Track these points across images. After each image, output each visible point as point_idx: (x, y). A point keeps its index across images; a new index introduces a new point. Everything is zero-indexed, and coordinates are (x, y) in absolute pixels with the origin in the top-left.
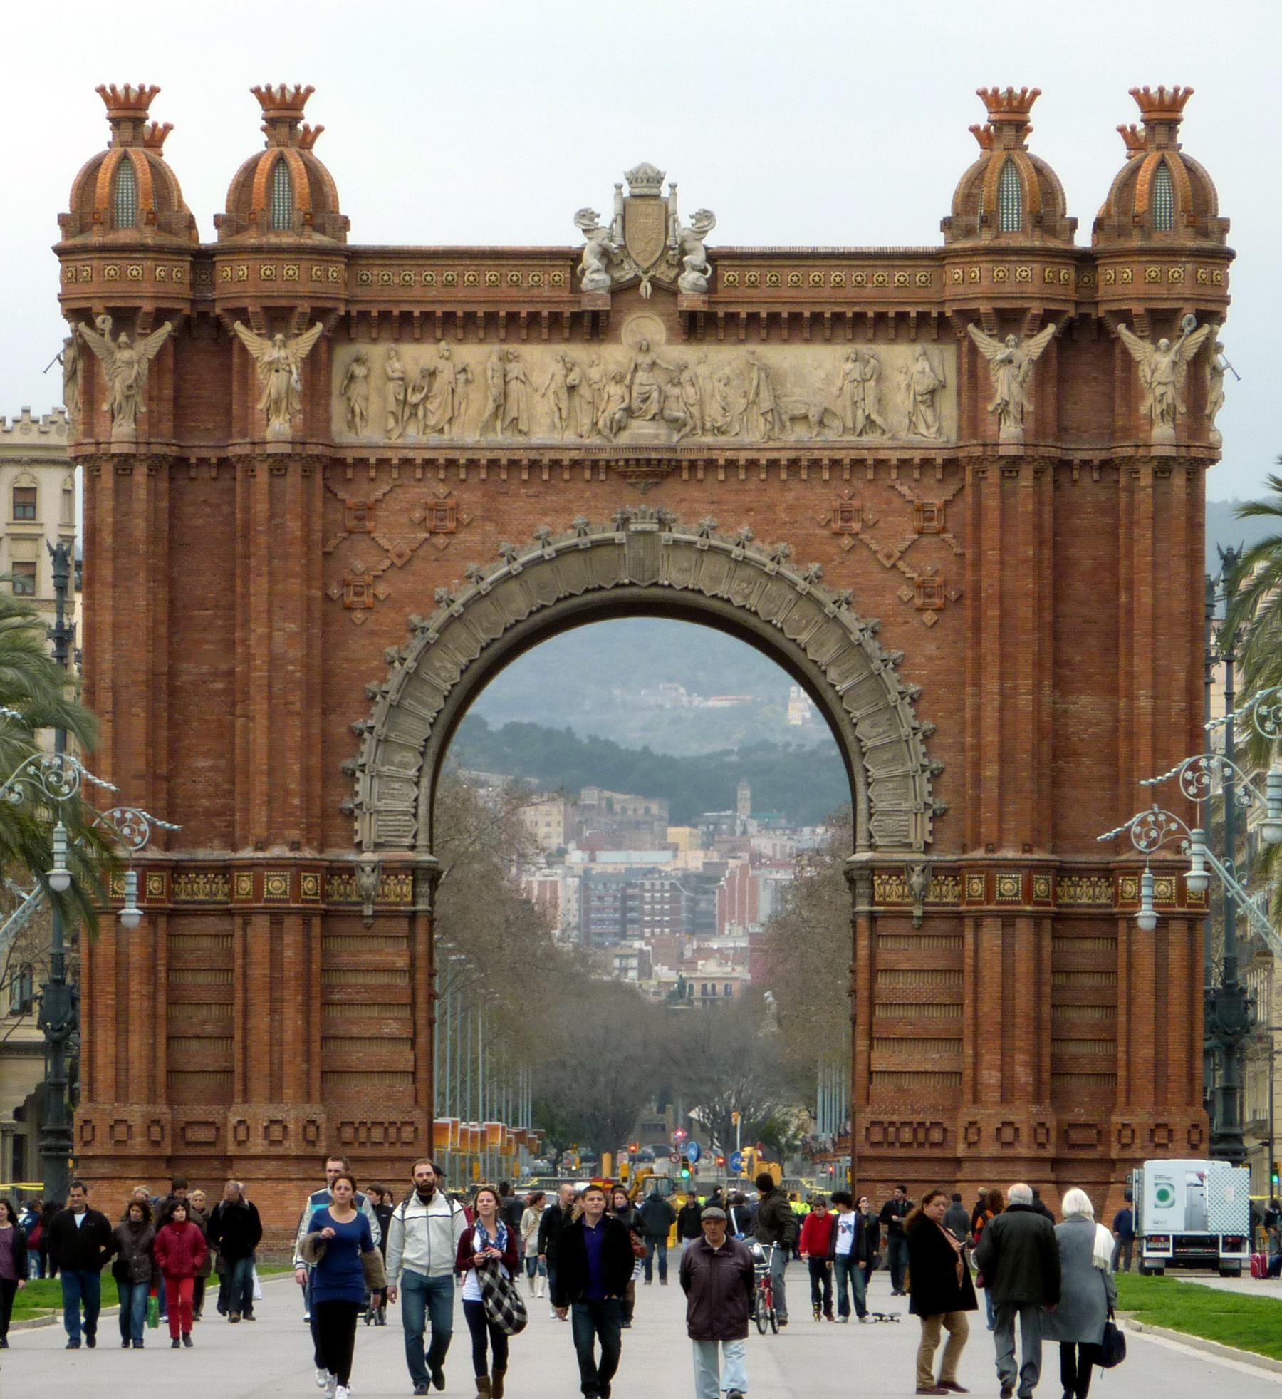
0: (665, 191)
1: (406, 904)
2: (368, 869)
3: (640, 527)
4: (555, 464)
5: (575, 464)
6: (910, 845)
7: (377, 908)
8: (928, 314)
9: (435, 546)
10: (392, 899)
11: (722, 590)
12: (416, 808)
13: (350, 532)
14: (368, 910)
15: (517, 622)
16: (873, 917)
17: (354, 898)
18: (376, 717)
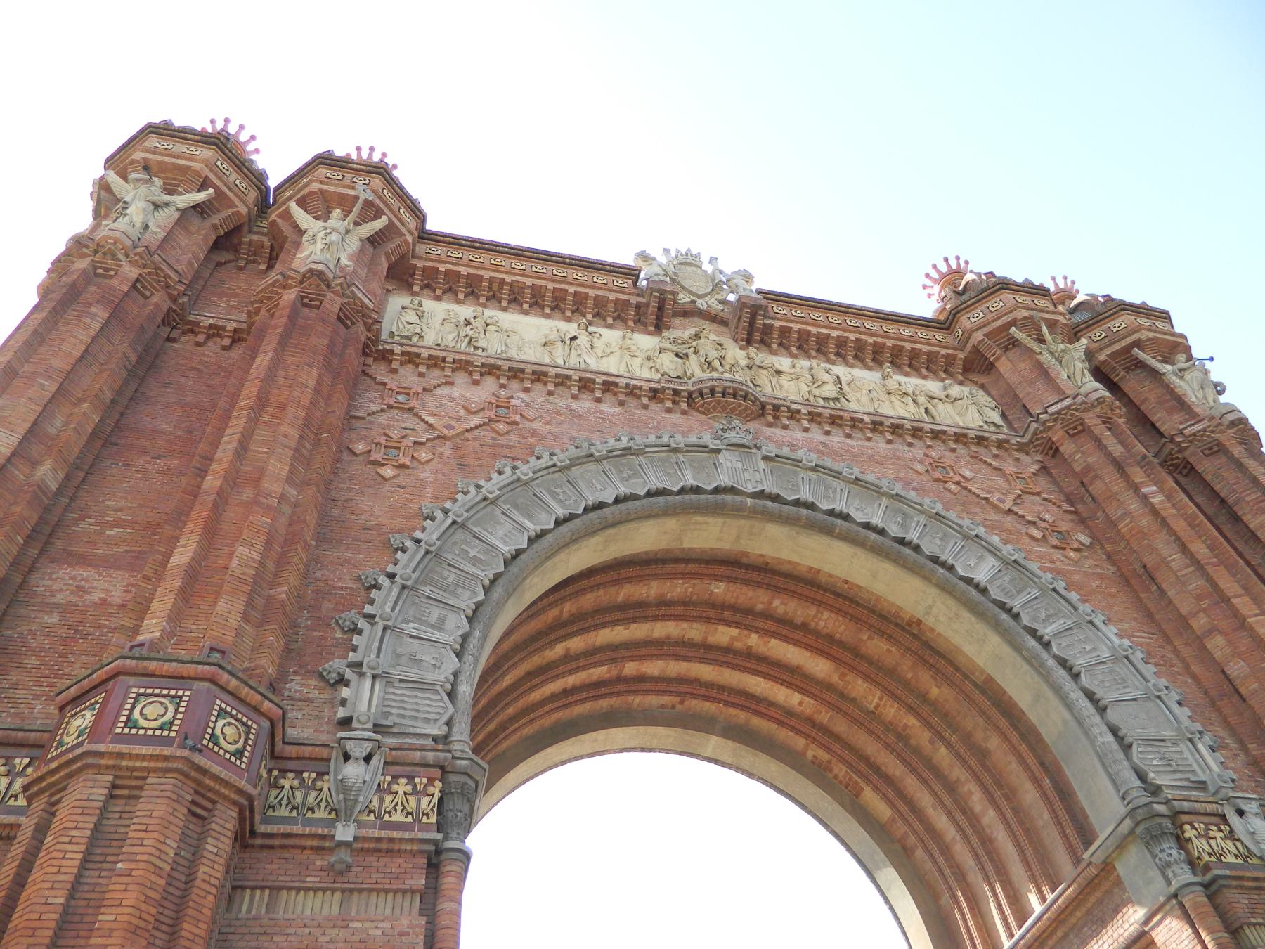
0: (708, 267)
1: (425, 828)
2: (358, 750)
3: (733, 441)
4: (632, 391)
5: (655, 394)
6: (1201, 786)
7: (363, 833)
8: (955, 357)
9: (494, 430)
10: (398, 817)
11: (839, 506)
12: (454, 685)
13: (390, 407)
14: (345, 832)
15: (600, 506)
16: (1212, 889)
17: (321, 814)
18: (405, 565)
